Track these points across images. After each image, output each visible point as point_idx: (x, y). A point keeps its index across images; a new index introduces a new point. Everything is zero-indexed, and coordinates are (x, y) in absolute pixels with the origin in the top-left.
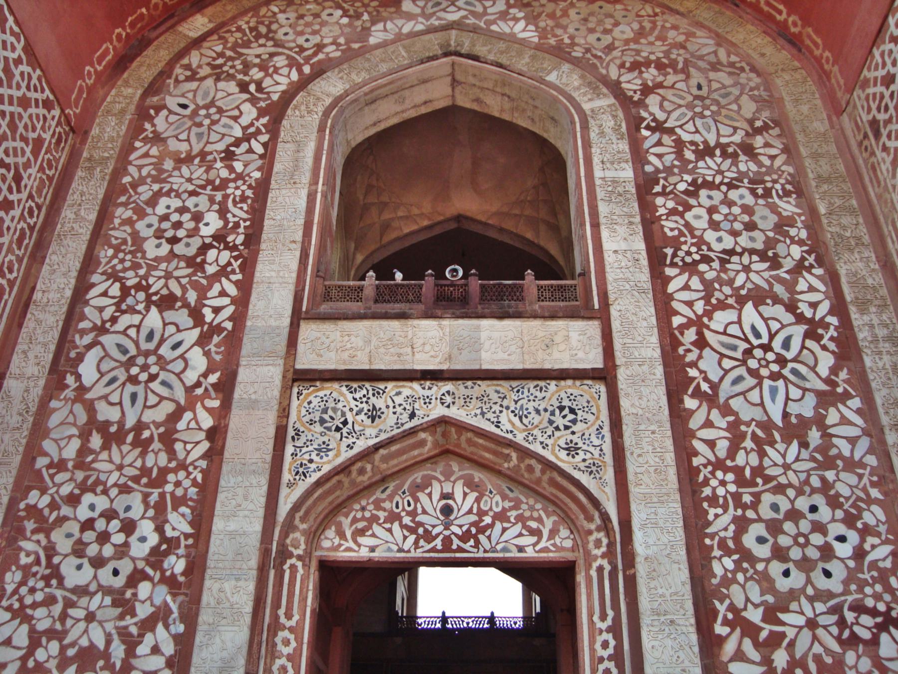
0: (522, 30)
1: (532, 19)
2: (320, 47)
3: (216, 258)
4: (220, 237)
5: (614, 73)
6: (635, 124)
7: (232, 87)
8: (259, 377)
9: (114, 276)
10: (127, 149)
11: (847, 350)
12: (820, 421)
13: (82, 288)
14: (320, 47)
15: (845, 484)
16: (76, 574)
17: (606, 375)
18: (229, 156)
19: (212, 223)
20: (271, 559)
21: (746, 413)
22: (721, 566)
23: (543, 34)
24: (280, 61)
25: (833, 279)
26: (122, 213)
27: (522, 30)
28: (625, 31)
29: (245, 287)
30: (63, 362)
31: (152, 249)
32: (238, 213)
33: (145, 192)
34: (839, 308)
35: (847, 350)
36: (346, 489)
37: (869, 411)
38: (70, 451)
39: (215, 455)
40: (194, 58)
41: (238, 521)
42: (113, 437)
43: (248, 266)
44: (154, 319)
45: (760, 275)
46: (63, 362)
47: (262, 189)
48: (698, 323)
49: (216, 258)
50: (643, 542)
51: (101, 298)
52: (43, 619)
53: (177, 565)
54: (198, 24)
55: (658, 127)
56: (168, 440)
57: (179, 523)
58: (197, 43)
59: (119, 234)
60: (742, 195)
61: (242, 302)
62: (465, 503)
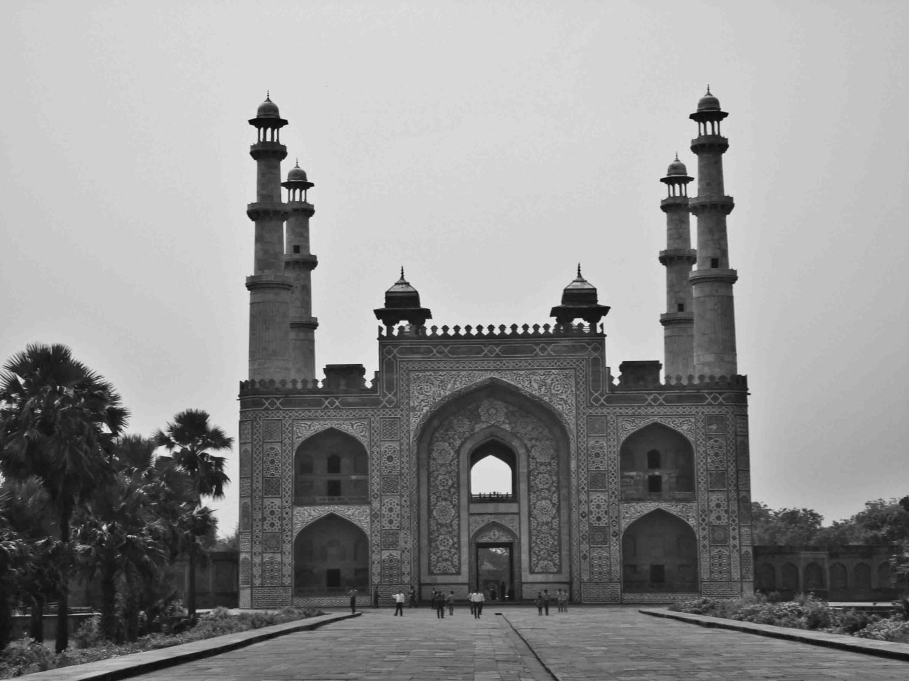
0: (507, 427)
1: (510, 423)
2: (464, 433)
3: (453, 490)
4: (452, 485)
5: (526, 442)
6: (529, 456)
7: (447, 444)
8: (464, 514)
9: (435, 494)
10: (429, 463)
11: (559, 510)
12: (551, 522)
13: (429, 497)
14: (464, 433)
15: (553, 532)
16: (442, 548)
17: (518, 514)
18: (451, 465)
19: (450, 482)
20: (470, 545)
21: (540, 520)
22: (533, 545)
23: (512, 428)
24: (456, 437)
25: (559, 495)
26: (432, 479)
27: (507, 427)
28: (529, 428)
29: (459, 496)
30: (430, 512)
31: (441, 488)
32: (455, 480)
33: (436, 473)
34: (559, 502)
35: (559, 510)
36: (480, 532)
37: (559, 521)
38: (435, 528)
39: (459, 528)
40: (437, 435)
41: (464, 539)
42: (442, 525)
43: (459, 492)
44: (444, 503)
45: (547, 494)
46: (430, 512)
47: (458, 473)
48: (535, 504)
49: (453, 490)
50: (522, 541)
51: (433, 499)
52: (438, 555)
53: (456, 546)
54: (436, 423)
55: (534, 458)
56: (451, 526)
57: (455, 540)
58: (436, 429)
59: (433, 484)
60: (546, 476)
61: (459, 499)
62: (497, 533)
